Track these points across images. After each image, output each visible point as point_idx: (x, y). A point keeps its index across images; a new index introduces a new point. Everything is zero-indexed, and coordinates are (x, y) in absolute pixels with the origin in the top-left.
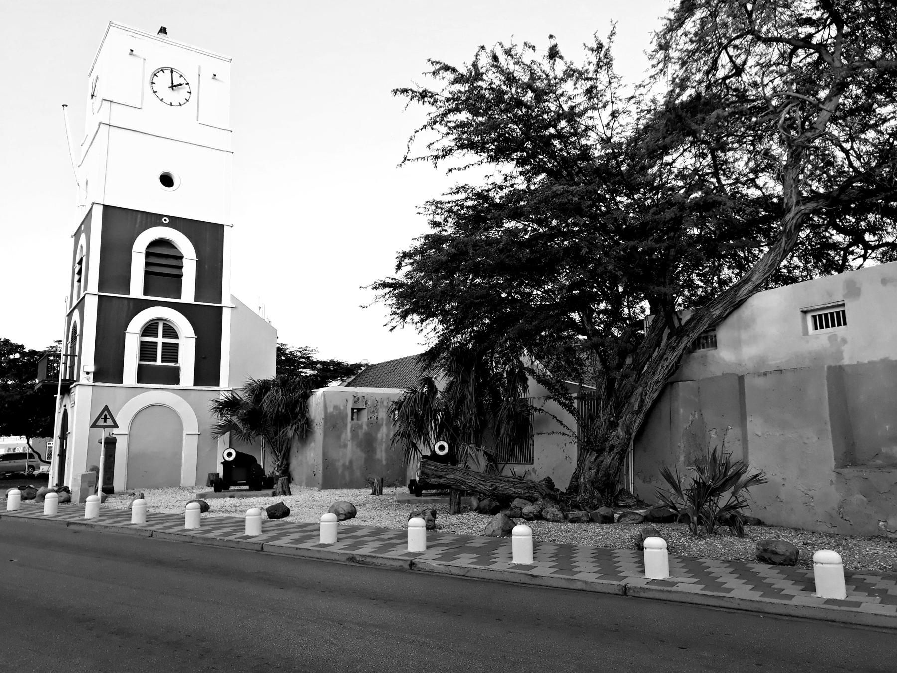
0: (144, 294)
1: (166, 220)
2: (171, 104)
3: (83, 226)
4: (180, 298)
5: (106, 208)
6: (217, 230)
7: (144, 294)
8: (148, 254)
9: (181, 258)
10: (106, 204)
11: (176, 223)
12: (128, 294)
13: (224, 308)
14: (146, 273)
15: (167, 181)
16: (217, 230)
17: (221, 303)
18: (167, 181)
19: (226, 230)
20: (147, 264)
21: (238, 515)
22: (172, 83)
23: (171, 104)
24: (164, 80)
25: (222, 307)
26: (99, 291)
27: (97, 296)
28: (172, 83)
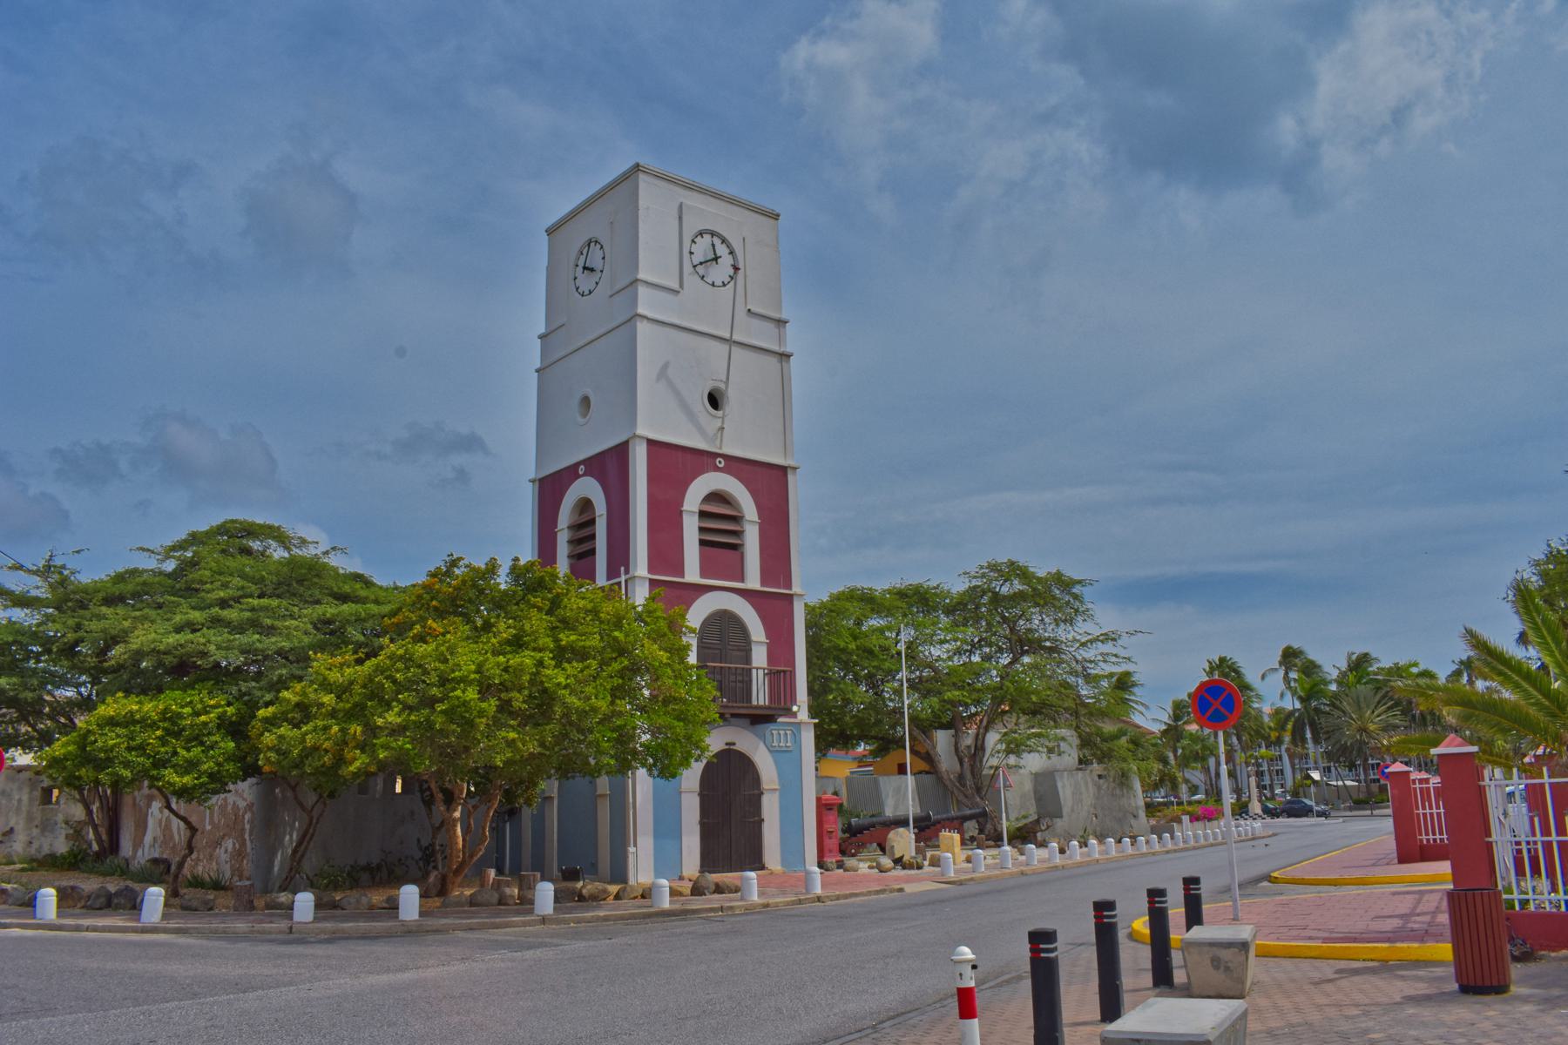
1: (720, 462)
2: (713, 285)
3: (582, 467)
4: (742, 580)
5: (651, 443)
8: (703, 515)
9: (736, 519)
11: (738, 466)
12: (683, 577)
13: (795, 598)
14: (702, 543)
15: (714, 400)
17: (791, 589)
18: (714, 400)
20: (702, 530)
21: (558, 905)
22: (715, 254)
23: (713, 285)
24: (702, 248)
25: (791, 596)
26: (651, 570)
27: (647, 584)
28: (715, 254)
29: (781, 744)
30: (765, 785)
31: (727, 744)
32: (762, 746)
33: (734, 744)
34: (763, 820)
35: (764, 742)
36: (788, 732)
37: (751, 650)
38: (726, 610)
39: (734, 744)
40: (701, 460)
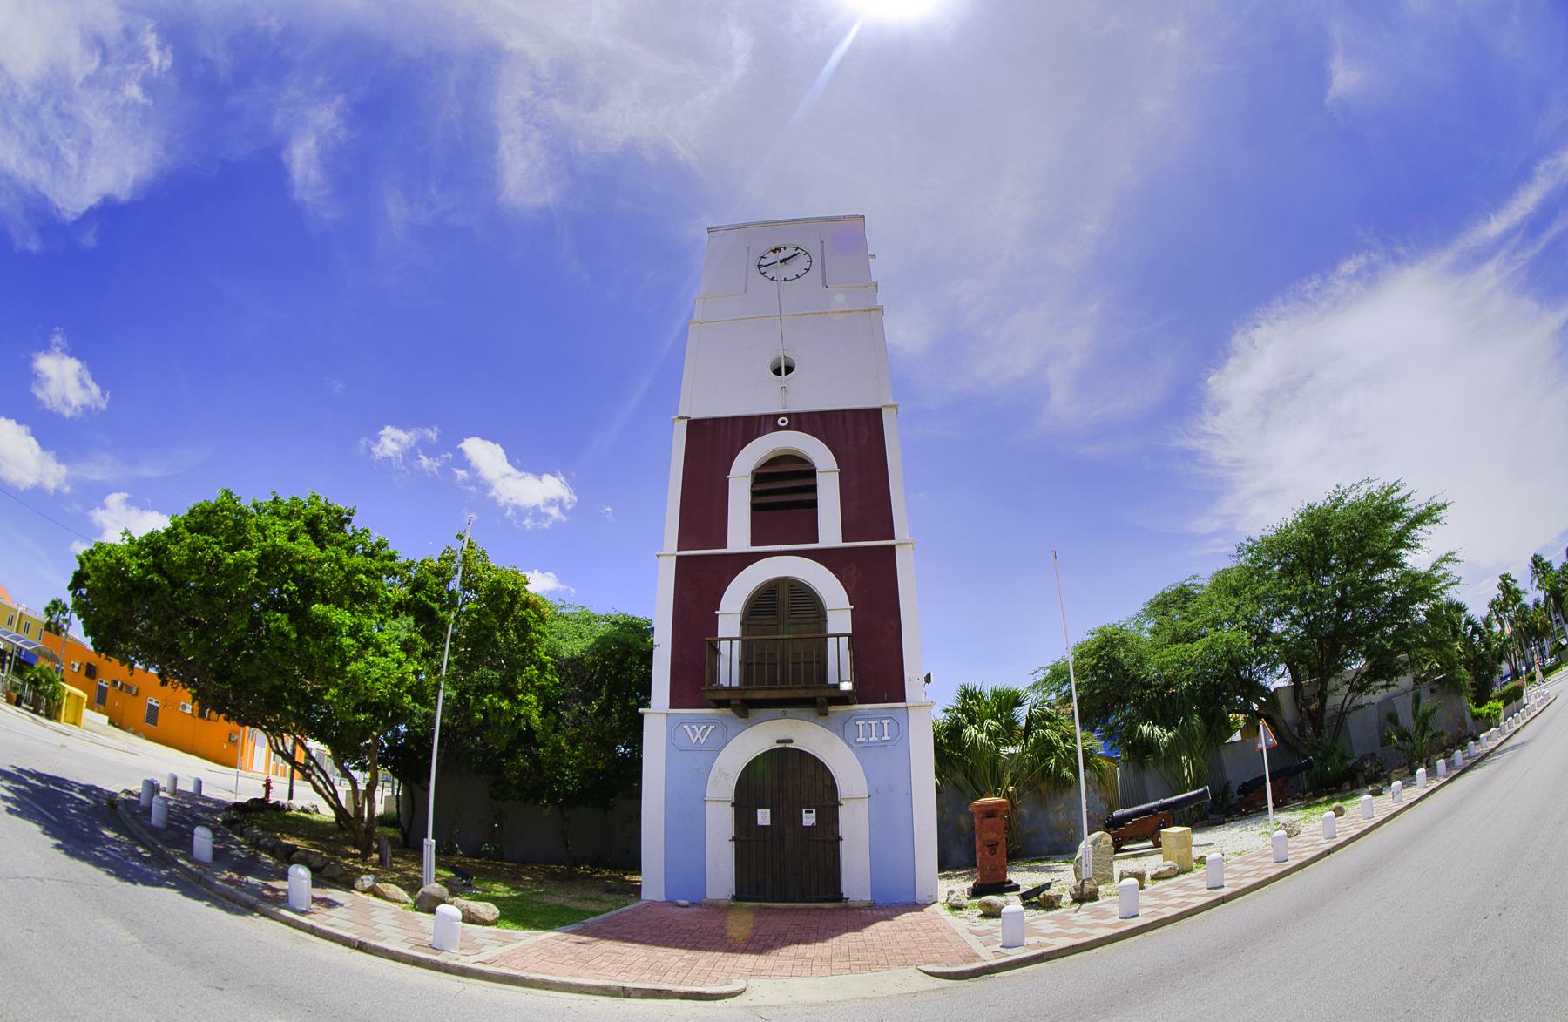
0: (752, 545)
1: (783, 422)
6: (871, 420)
7: (752, 545)
10: (694, 416)
11: (800, 422)
12: (726, 547)
14: (755, 508)
16: (871, 420)
19: (888, 420)
29: (873, 738)
30: (843, 790)
31: (779, 742)
32: (838, 740)
33: (791, 741)
34: (840, 839)
35: (844, 739)
36: (885, 722)
37: (826, 621)
38: (786, 579)
39: (791, 741)
40: (753, 426)
